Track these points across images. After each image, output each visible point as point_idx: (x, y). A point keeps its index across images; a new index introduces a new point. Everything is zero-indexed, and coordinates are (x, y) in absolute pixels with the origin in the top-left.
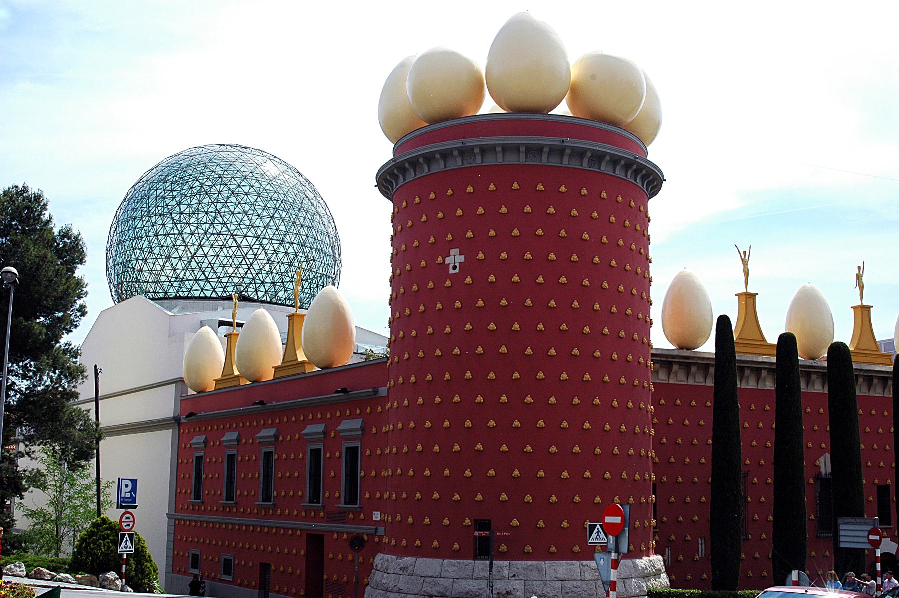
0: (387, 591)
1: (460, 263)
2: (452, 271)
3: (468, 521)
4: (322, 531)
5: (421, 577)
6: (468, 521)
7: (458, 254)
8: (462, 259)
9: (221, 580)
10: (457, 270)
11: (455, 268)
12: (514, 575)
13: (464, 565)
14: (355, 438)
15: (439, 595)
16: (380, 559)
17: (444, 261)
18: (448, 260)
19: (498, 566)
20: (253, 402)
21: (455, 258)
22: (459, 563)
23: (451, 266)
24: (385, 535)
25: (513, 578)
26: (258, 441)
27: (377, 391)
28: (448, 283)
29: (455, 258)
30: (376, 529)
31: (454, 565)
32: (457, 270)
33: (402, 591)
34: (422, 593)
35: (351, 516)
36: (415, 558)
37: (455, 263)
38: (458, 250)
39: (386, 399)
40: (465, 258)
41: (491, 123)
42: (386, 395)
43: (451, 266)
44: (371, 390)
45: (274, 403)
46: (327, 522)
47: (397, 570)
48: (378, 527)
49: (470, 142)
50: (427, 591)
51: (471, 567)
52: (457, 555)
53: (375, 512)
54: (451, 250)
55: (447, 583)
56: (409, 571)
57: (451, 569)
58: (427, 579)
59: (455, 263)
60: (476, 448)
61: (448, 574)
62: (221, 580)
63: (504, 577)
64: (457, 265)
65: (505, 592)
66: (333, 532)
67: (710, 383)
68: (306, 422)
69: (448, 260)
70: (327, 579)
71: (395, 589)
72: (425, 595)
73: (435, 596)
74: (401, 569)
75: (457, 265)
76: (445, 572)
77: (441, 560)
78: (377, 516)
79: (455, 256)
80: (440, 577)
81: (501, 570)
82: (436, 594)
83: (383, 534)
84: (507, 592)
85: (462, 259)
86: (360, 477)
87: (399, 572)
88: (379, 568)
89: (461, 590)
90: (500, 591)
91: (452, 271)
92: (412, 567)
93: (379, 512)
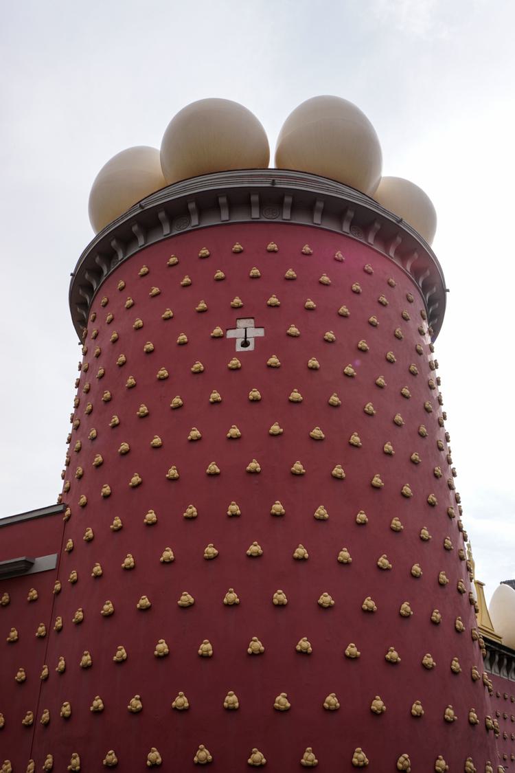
1: (257, 339)
2: (239, 348)
7: (253, 325)
8: (260, 333)
10: (251, 348)
11: (245, 344)
18: (231, 334)
21: (246, 331)
23: (239, 342)
27: (32, 564)
28: (235, 362)
32: (251, 348)
37: (246, 338)
38: (252, 320)
39: (55, 573)
43: (239, 342)
44: (23, 558)
49: (281, 183)
54: (238, 321)
59: (246, 338)
60: (298, 648)
64: (252, 341)
69: (231, 334)
75: (252, 341)
79: (246, 329)
85: (260, 333)
91: (239, 348)
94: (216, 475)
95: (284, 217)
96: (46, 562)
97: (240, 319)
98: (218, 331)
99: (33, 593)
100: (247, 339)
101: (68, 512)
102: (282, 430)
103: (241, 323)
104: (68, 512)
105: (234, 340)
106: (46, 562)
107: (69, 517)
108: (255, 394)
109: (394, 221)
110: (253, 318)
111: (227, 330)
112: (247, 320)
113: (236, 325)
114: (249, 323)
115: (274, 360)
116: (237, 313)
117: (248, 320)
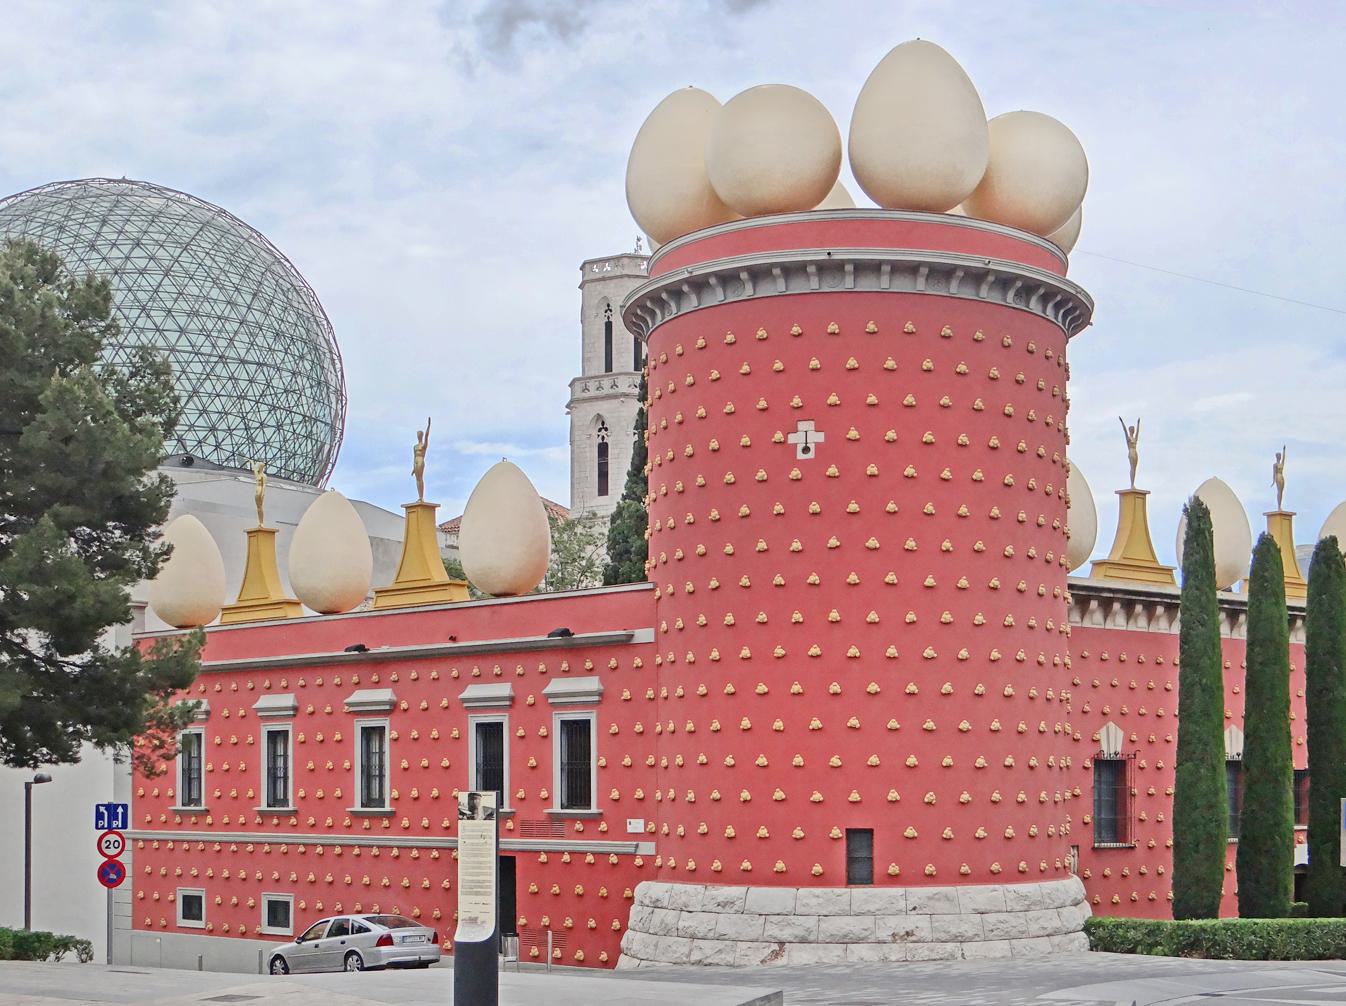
0: (693, 937)
1: (817, 445)
2: (800, 456)
3: (836, 832)
4: (511, 851)
6: (836, 832)
7: (813, 428)
8: (820, 437)
9: (261, 936)
10: (811, 455)
11: (806, 450)
12: (914, 909)
14: (585, 705)
16: (645, 890)
17: (786, 438)
18: (792, 439)
20: (358, 643)
21: (807, 435)
24: (657, 853)
25: (913, 912)
26: (346, 709)
28: (795, 473)
29: (807, 435)
30: (637, 846)
31: (818, 897)
32: (811, 455)
33: (726, 937)
34: (768, 939)
35: (579, 826)
36: (742, 889)
38: (812, 422)
39: (654, 647)
40: (826, 436)
41: (852, 226)
45: (385, 649)
46: (522, 836)
47: (711, 907)
50: (775, 935)
51: (846, 898)
52: (819, 880)
53: (632, 820)
55: (811, 922)
56: (736, 908)
57: (814, 902)
62: (261, 936)
63: (901, 911)
65: (903, 933)
66: (538, 852)
67: (1176, 629)
68: (460, 682)
69: (792, 439)
71: (711, 935)
75: (812, 447)
77: (792, 890)
78: (636, 825)
81: (894, 901)
82: (792, 940)
83: (654, 853)
84: (907, 933)
85: (820, 437)
88: (665, 904)
89: (835, 933)
90: (896, 931)
91: (800, 456)
93: (641, 822)
96: (644, 635)
98: (779, 436)
99: (638, 662)
103: (803, 426)
106: (644, 635)
107: (660, 598)
113: (797, 427)
114: (808, 426)
115: (833, 470)
116: (797, 413)
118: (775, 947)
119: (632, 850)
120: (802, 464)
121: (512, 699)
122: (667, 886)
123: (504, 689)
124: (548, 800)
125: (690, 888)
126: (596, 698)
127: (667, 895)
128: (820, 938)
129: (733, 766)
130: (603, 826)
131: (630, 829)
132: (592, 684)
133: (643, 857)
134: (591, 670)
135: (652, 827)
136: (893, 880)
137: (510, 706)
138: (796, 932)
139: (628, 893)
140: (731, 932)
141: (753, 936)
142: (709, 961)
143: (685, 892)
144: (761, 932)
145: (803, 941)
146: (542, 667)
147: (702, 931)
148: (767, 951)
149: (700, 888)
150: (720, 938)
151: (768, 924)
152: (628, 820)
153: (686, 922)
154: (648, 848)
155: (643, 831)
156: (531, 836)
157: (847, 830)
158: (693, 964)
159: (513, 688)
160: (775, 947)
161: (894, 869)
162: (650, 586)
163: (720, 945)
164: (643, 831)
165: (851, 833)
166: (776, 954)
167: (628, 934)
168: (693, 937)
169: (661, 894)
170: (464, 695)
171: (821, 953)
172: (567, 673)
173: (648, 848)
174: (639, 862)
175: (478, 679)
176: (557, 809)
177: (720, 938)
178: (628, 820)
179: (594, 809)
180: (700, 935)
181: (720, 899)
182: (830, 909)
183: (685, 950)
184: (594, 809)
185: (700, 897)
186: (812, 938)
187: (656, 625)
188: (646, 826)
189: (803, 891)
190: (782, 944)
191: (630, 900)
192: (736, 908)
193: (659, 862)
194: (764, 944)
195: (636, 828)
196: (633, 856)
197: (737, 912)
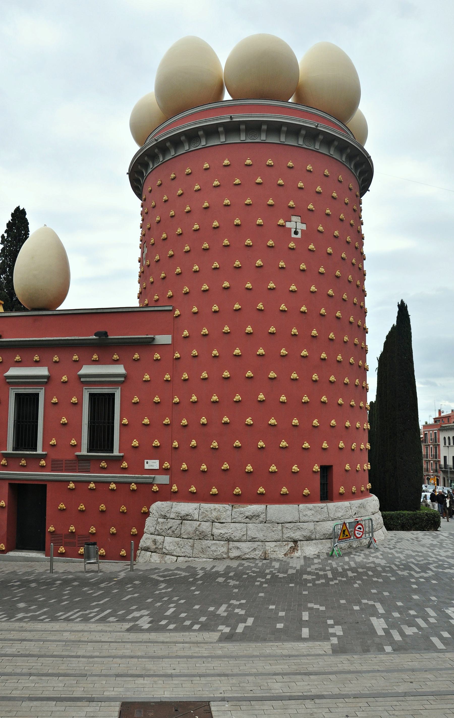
1: (302, 230)
2: (293, 236)
5: (279, 523)
6: (316, 468)
7: (300, 221)
8: (304, 227)
10: (299, 236)
11: (296, 233)
12: (355, 513)
13: (319, 509)
15: (304, 539)
18: (288, 225)
19: (346, 507)
22: (315, 507)
28: (292, 245)
32: (299, 236)
37: (296, 229)
38: (299, 218)
42: (170, 342)
43: (293, 230)
48: (156, 476)
52: (306, 499)
53: (148, 461)
55: (311, 526)
57: (309, 513)
58: (287, 525)
59: (296, 229)
61: (306, 519)
66: (68, 482)
69: (288, 225)
70: (52, 533)
71: (244, 538)
72: (288, 541)
73: (301, 541)
74: (247, 517)
76: (304, 517)
79: (296, 222)
80: (300, 522)
81: (347, 510)
82: (301, 539)
86: (123, 426)
87: (243, 521)
89: (326, 532)
92: (264, 514)
94: (285, 311)
95: (316, 148)
97: (293, 215)
98: (281, 222)
99: (157, 356)
100: (297, 230)
101: (177, 312)
102: (316, 290)
103: (294, 218)
104: (177, 312)
105: (290, 229)
108: (303, 266)
109: (367, 157)
110: (300, 216)
111: (286, 221)
112: (296, 217)
116: (292, 211)
117: (297, 217)
118: (292, 544)
119: (150, 480)
120: (295, 240)
121: (48, 377)
122: (196, 505)
123: (43, 371)
124: (77, 447)
125: (217, 506)
126: (123, 379)
127: (196, 512)
128: (317, 537)
129: (251, 425)
130: (125, 464)
131: (147, 467)
132: (120, 369)
133: (158, 485)
134: (118, 360)
135: (167, 465)
136: (342, 497)
137: (46, 382)
138: (305, 534)
139: (145, 509)
140: (260, 536)
141: (276, 537)
142: (247, 556)
143: (215, 509)
144: (281, 535)
145: (309, 539)
146: (75, 357)
147: (237, 535)
148: (287, 548)
149: (228, 507)
150: (253, 540)
151: (284, 529)
152: (146, 461)
153: (218, 530)
154: (164, 479)
155: (157, 467)
156: (62, 471)
157: (320, 466)
158: (232, 559)
159: (49, 370)
160: (292, 544)
161: (342, 490)
162: (171, 308)
163: (255, 545)
164: (157, 467)
165: (322, 467)
166: (294, 549)
167: (145, 536)
168: (229, 540)
169: (191, 511)
170: (8, 373)
171: (320, 546)
172: (95, 362)
173: (164, 479)
174: (155, 488)
175: (18, 364)
176: (84, 452)
177: (253, 540)
178: (146, 461)
179: (116, 452)
180: (235, 539)
181: (247, 514)
182: (319, 517)
183: (225, 549)
184: (116, 452)
185: (229, 513)
186: (313, 537)
187: (175, 333)
188: (161, 464)
189: (301, 506)
190: (295, 542)
191: (147, 514)
192: (261, 519)
193: (175, 488)
194: (285, 543)
195: (152, 466)
196: (152, 484)
197: (261, 522)
